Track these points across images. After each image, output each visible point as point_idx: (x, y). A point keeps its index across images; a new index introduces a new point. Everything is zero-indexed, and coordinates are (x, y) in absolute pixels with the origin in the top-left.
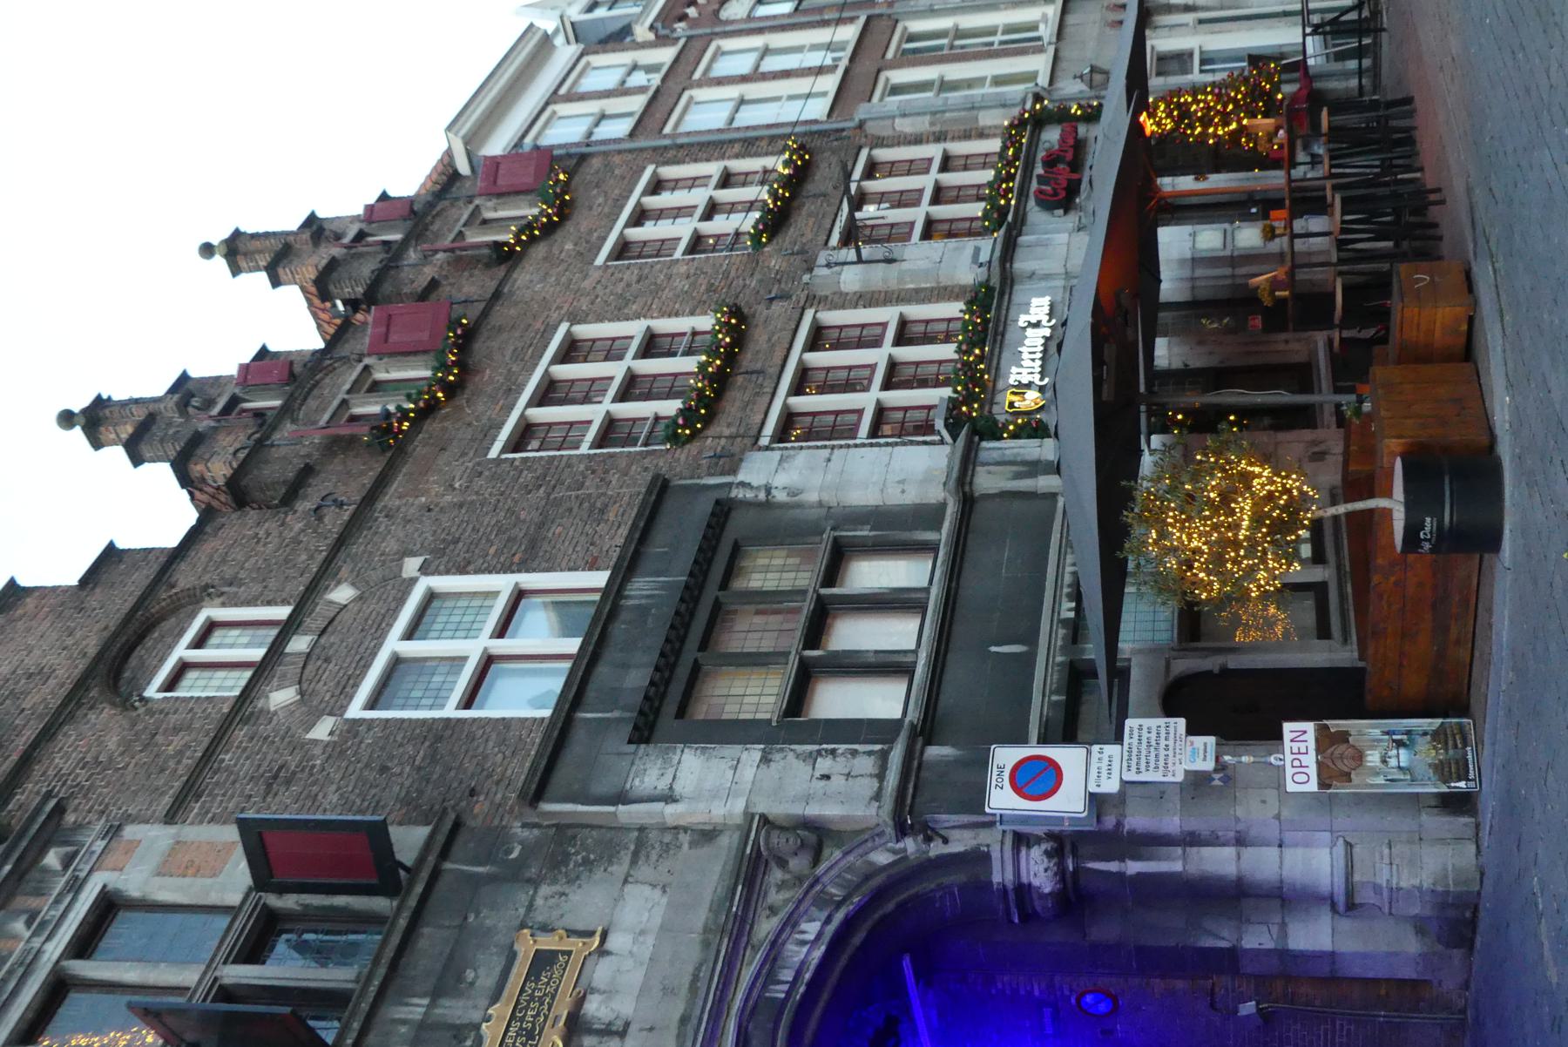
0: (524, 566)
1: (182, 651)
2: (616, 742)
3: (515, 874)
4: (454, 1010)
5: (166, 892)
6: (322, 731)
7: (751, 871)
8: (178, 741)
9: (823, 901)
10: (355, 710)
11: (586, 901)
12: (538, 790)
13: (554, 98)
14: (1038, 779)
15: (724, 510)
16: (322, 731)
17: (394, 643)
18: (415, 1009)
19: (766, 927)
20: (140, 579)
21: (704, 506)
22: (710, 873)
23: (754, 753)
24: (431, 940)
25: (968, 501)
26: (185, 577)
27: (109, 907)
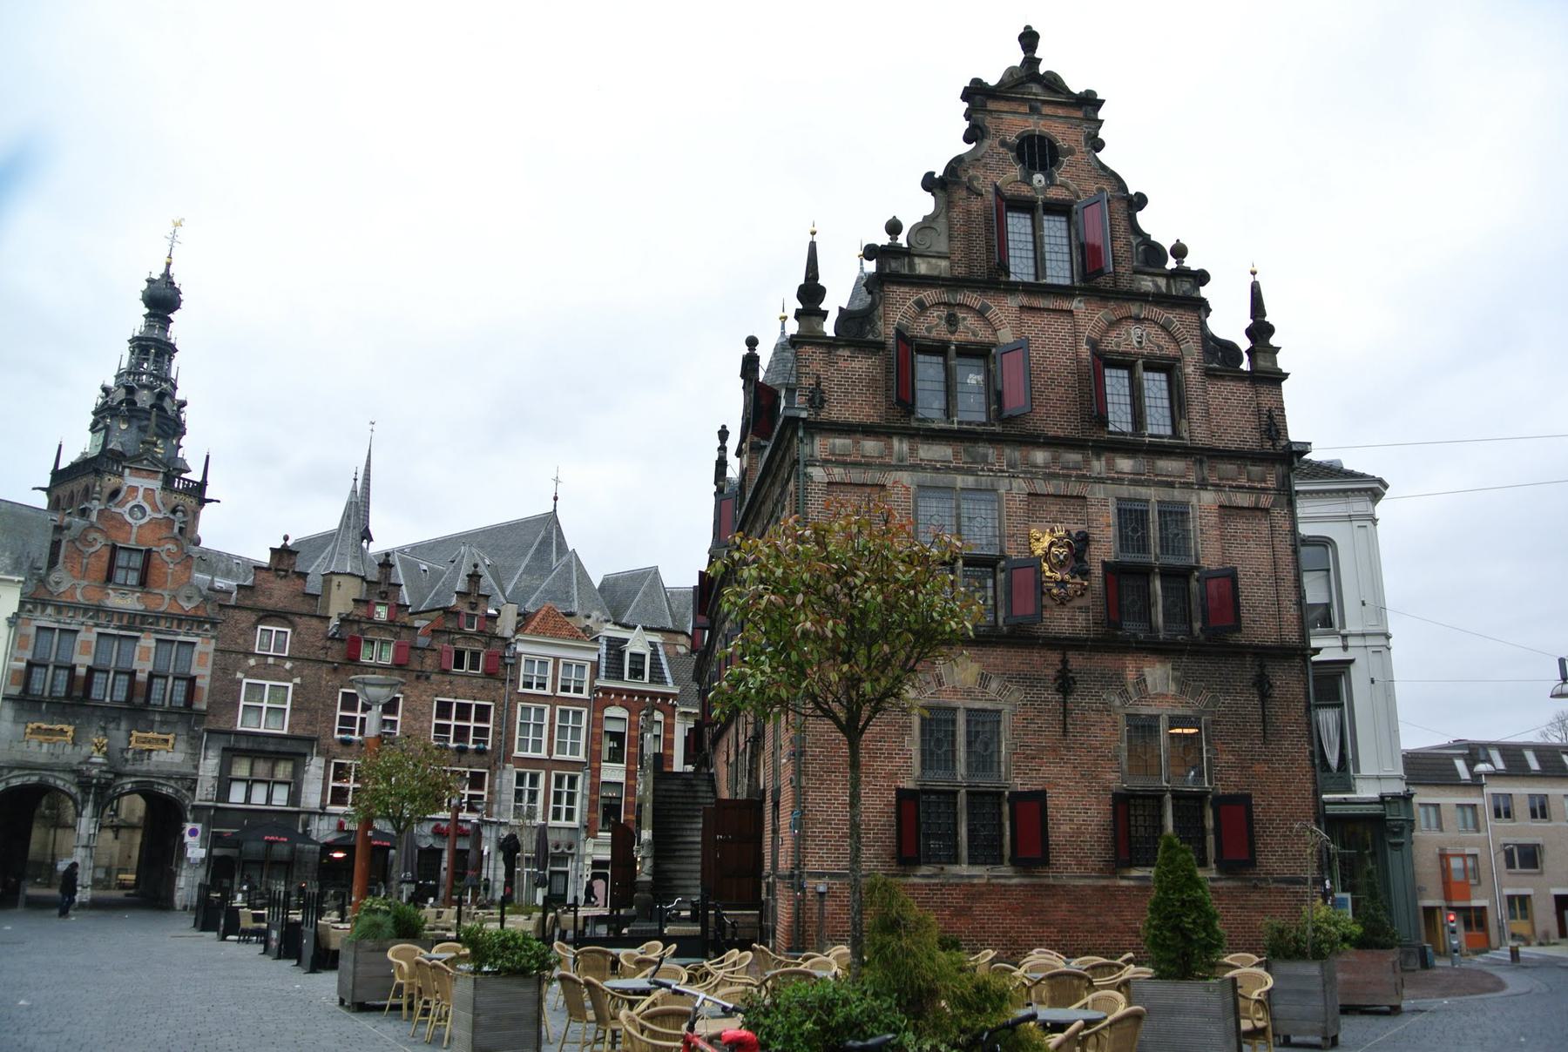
0: (292, 709)
1: (275, 629)
2: (223, 744)
3: (190, 729)
4: (156, 725)
5: (196, 656)
6: (239, 675)
7: (183, 778)
8: (240, 641)
9: (177, 791)
10: (245, 681)
11: (181, 746)
12: (210, 732)
13: (557, 659)
14: (193, 833)
15: (305, 755)
16: (239, 675)
17: (268, 683)
18: (158, 718)
19: (172, 783)
20: (305, 608)
21: (304, 750)
22: (187, 769)
23: (216, 774)
24: (175, 717)
25: (298, 813)
26: (302, 623)
27: (194, 644)
